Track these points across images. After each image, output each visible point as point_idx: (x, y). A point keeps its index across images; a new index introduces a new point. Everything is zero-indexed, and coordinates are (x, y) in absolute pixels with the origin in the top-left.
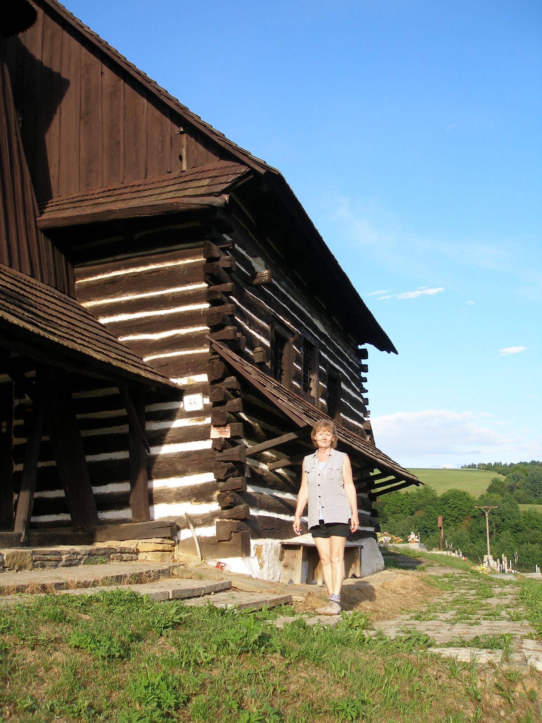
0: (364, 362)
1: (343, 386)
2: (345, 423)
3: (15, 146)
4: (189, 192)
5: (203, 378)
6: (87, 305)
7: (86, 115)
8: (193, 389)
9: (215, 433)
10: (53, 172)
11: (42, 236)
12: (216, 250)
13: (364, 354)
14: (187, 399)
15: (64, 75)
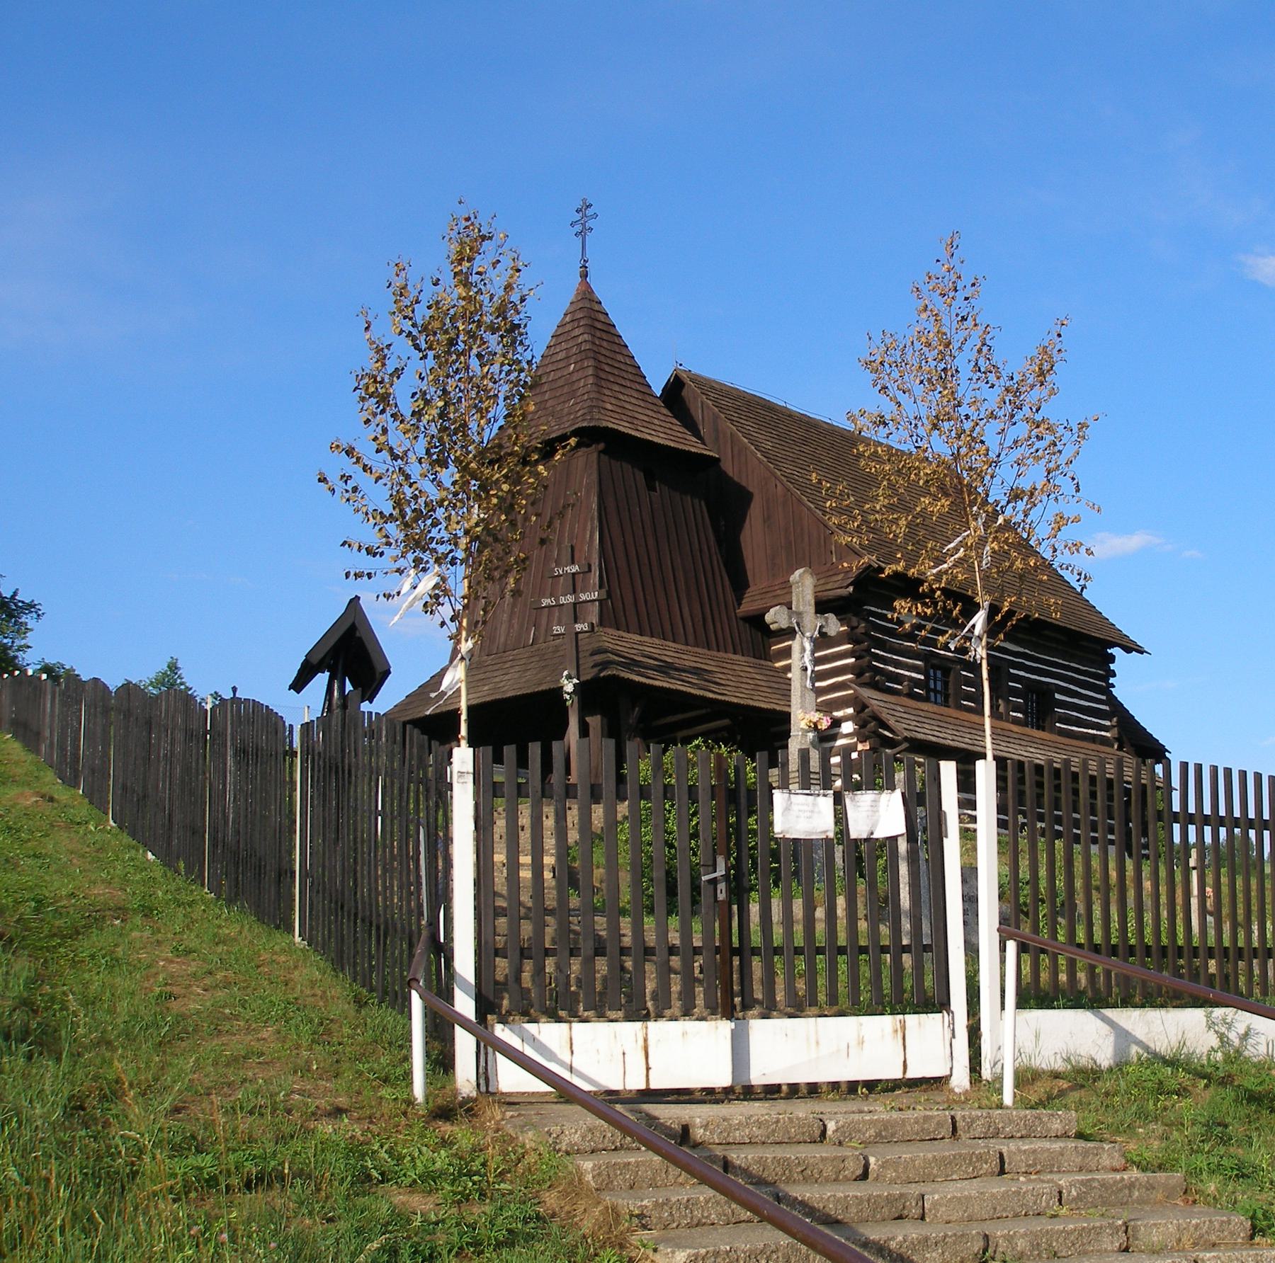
0: (1112, 666)
1: (1057, 696)
2: (1062, 733)
3: (715, 563)
4: (829, 587)
5: (850, 711)
6: (778, 665)
7: (767, 519)
8: (846, 719)
9: (860, 747)
10: (749, 566)
11: (741, 623)
12: (854, 621)
13: (1112, 659)
14: (843, 725)
15: (751, 489)
